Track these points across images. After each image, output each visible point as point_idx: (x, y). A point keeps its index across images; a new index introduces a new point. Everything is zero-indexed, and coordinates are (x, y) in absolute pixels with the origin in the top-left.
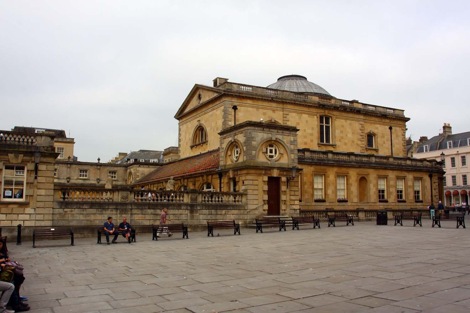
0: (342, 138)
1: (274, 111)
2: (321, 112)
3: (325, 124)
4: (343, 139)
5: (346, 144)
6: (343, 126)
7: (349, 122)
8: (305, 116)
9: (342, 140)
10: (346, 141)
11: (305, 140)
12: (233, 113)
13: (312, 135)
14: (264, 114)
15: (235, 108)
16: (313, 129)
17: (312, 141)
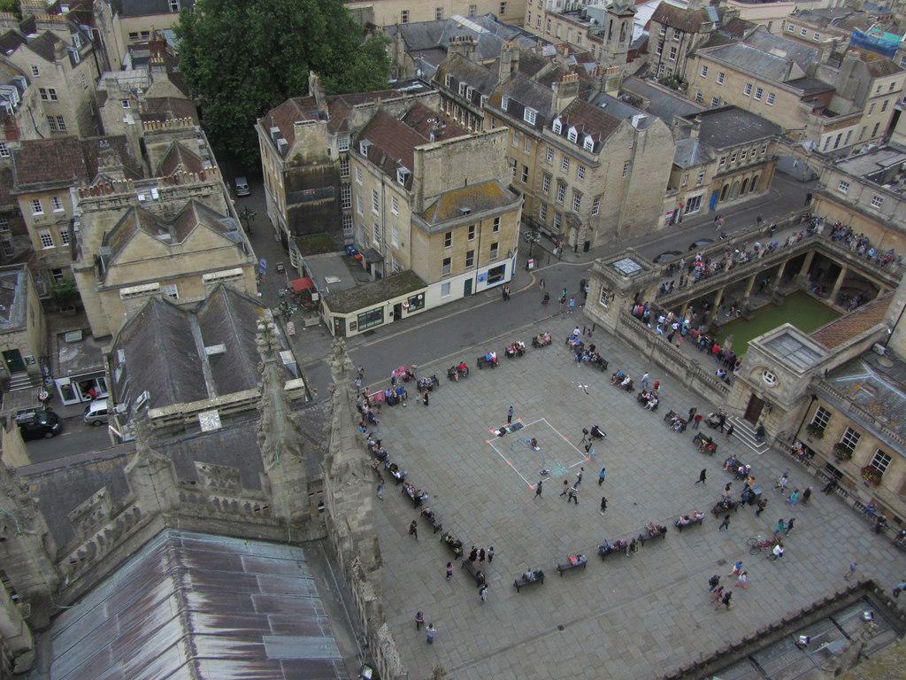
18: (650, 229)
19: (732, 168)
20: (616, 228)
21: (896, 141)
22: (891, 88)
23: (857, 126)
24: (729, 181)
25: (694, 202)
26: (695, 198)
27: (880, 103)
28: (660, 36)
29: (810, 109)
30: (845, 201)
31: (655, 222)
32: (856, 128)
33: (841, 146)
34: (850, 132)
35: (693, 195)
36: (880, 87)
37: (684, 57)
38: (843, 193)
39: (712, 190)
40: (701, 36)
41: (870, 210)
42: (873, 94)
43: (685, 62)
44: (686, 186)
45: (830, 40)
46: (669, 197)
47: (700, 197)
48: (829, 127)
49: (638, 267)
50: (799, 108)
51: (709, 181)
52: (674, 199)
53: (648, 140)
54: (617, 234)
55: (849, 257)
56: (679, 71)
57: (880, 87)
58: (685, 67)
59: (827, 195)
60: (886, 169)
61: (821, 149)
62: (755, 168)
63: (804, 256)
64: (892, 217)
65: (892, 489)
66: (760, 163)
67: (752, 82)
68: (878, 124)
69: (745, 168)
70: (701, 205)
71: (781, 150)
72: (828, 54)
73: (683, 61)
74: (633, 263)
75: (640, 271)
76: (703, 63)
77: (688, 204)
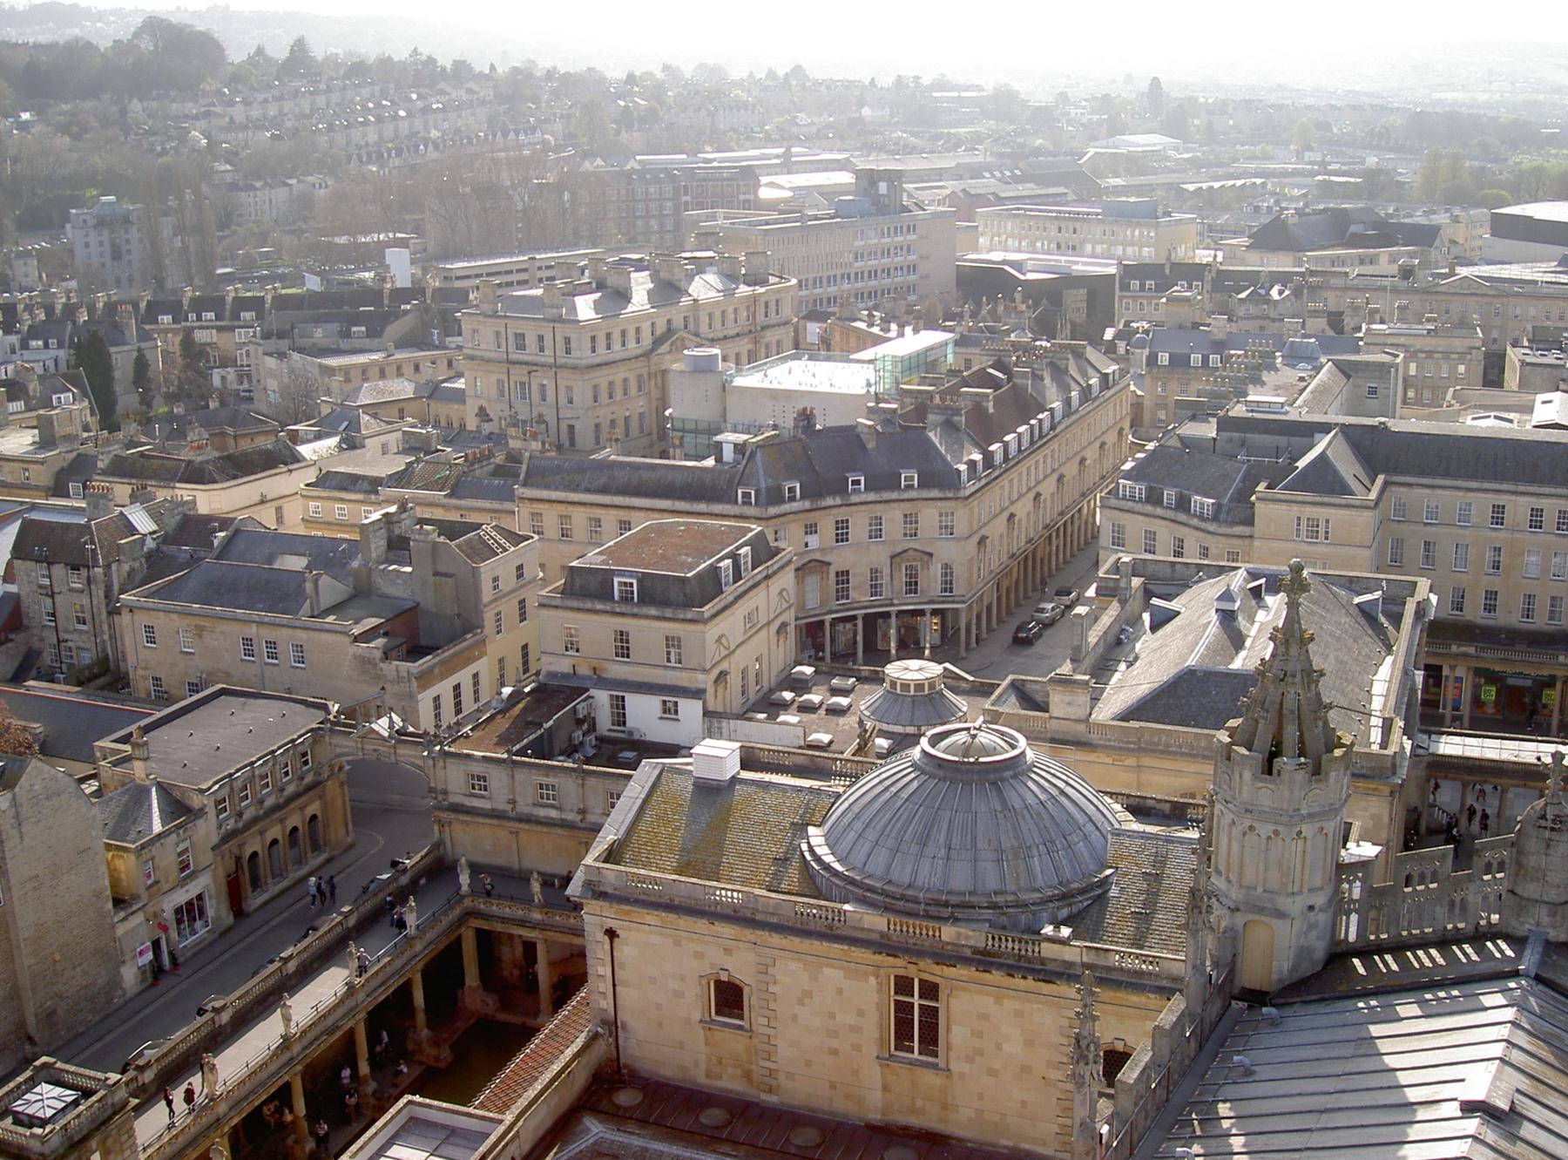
1: (728, 951)
2: (899, 965)
3: (920, 997)
4: (982, 1055)
5: (992, 1072)
6: (984, 1017)
7: (1010, 1005)
8: (833, 974)
9: (978, 1059)
10: (997, 1065)
11: (835, 1043)
12: (607, 947)
13: (857, 1029)
14: (699, 955)
15: (611, 934)
16: (861, 1013)
17: (857, 1047)
18: (109, 1001)
19: (247, 815)
20: (22, 1024)
21: (552, 668)
22: (520, 576)
23: (485, 659)
24: (254, 845)
25: (191, 912)
26: (190, 904)
27: (509, 608)
28: (41, 587)
29: (378, 654)
30: (493, 810)
31: (115, 982)
32: (484, 666)
33: (469, 706)
34: (476, 676)
35: (182, 897)
36: (495, 579)
37: (104, 614)
38: (483, 797)
39: (221, 874)
40: (126, 567)
41: (542, 812)
42: (487, 593)
43: (111, 626)
44: (157, 882)
45: (376, 516)
46: (125, 919)
47: (200, 897)
48: (425, 679)
49: (70, 1095)
50: (355, 657)
51: (207, 857)
52: (139, 918)
53: (24, 810)
54: (30, 1039)
55: (537, 916)
56: (104, 649)
57: (495, 579)
58: (113, 637)
59: (457, 809)
60: (546, 726)
61: (427, 722)
62: (304, 798)
63: (455, 947)
64: (583, 812)
66: (309, 789)
67: (252, 630)
68: (525, 647)
69: (277, 808)
70: (210, 912)
71: (338, 750)
72: (383, 543)
73: (105, 628)
74: (58, 1091)
75: (76, 1103)
76: (142, 619)
77: (179, 921)
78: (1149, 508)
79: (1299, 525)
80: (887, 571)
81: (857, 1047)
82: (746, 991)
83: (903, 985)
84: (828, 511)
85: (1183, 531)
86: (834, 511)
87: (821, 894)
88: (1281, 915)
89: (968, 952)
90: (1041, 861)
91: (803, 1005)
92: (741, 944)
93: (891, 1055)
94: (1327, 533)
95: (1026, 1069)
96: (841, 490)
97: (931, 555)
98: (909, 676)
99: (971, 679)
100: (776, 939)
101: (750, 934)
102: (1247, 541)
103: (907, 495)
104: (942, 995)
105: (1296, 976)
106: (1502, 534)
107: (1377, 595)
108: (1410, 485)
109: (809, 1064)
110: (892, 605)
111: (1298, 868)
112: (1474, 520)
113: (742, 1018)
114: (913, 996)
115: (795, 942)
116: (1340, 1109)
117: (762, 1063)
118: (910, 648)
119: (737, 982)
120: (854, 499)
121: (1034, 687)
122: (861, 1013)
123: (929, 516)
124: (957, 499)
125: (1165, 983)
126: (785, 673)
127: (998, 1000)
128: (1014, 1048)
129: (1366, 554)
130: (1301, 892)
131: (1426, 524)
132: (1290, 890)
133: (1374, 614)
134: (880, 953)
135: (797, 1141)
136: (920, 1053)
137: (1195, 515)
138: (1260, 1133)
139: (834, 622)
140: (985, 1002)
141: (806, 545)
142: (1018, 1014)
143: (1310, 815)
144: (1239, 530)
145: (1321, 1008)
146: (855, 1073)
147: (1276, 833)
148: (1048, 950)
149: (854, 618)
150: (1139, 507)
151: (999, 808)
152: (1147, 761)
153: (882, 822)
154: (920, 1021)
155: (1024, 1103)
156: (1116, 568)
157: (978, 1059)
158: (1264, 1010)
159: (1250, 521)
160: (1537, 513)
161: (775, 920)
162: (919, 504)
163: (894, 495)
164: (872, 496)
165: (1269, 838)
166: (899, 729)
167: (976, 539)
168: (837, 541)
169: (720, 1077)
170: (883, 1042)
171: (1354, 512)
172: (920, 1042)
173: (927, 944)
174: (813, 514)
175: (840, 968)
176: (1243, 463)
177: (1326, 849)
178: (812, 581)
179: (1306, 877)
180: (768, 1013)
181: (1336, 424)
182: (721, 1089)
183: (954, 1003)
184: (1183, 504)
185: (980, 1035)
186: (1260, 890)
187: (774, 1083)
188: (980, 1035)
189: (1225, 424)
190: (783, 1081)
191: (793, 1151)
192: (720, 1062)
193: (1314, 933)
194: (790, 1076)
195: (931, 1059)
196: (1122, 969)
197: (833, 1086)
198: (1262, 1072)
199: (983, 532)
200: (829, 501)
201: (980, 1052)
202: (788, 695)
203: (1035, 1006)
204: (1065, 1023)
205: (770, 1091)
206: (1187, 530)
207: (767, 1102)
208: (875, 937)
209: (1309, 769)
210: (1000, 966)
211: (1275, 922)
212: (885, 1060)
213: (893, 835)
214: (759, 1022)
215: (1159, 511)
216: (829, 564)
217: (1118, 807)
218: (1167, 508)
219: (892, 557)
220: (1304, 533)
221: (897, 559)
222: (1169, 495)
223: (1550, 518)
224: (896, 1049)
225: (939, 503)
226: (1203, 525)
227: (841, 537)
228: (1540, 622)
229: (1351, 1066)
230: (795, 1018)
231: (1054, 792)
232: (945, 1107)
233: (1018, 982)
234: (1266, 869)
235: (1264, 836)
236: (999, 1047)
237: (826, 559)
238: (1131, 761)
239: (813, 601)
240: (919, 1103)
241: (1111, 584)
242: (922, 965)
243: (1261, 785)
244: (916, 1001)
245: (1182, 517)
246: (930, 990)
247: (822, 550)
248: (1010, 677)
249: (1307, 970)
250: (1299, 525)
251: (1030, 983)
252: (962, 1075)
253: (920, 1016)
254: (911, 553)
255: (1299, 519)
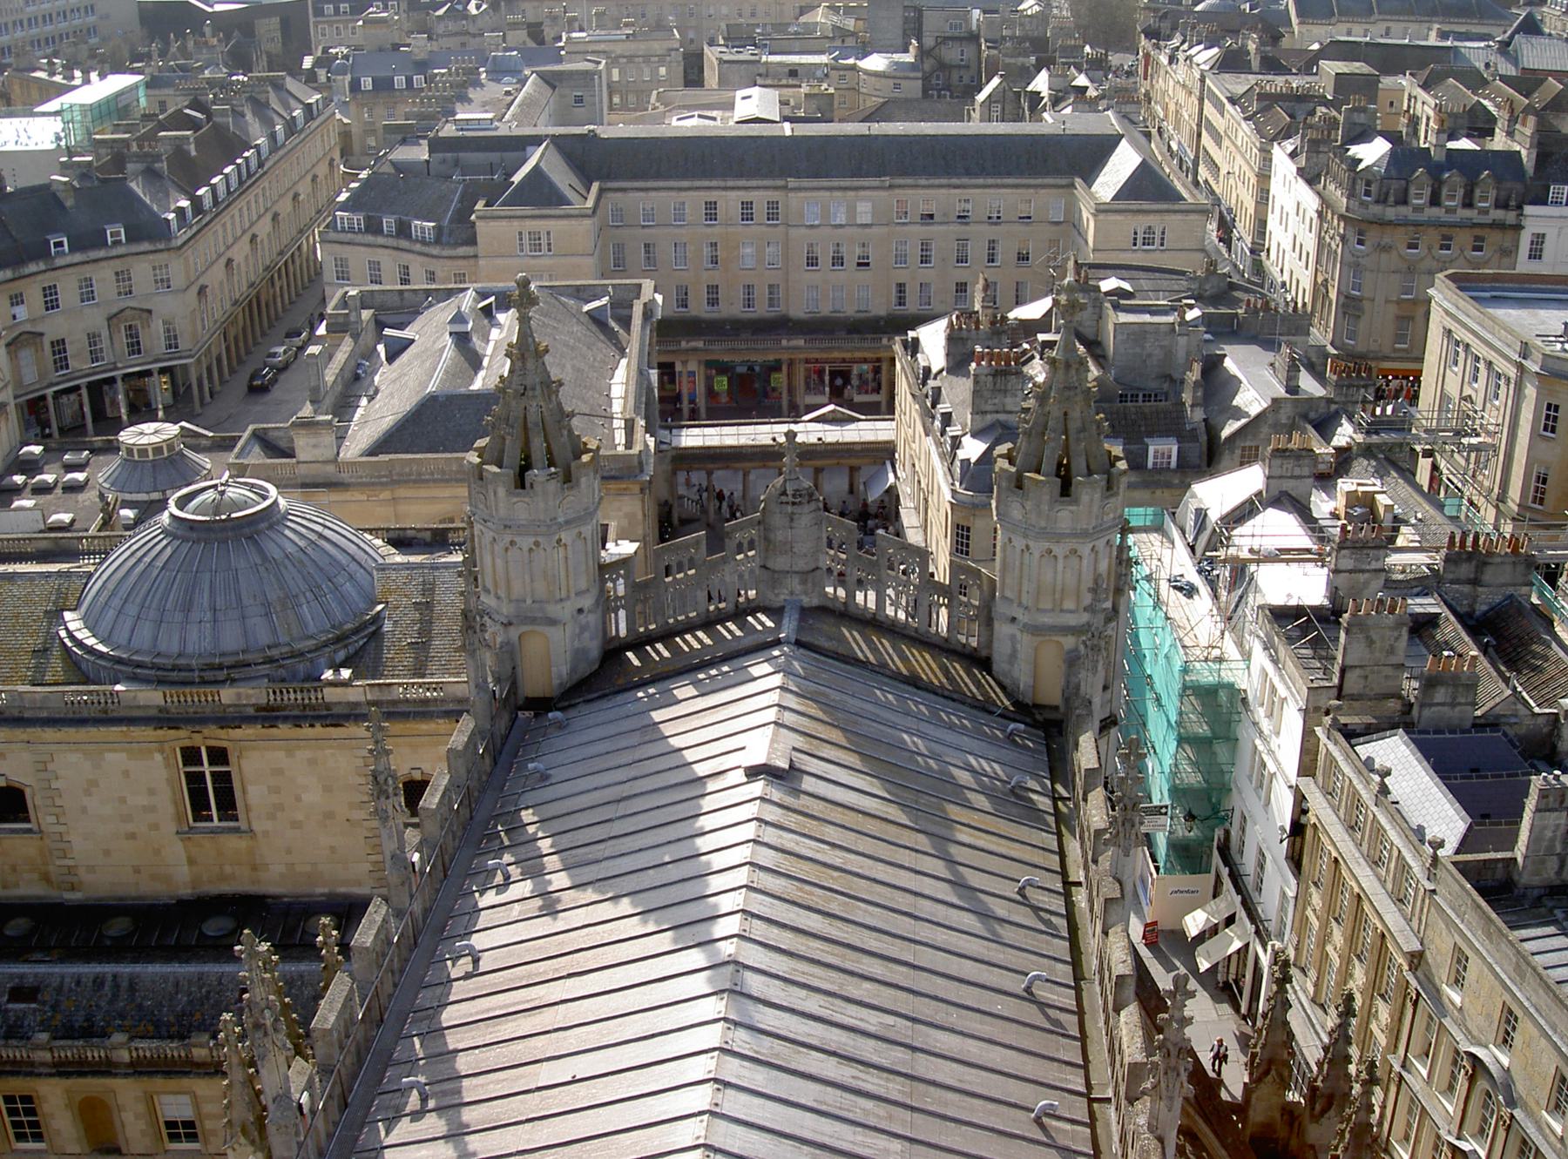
0: (280, 807)
3: (211, 764)
5: (296, 825)
6: (279, 772)
7: (303, 755)
8: (116, 759)
9: (279, 814)
10: (300, 817)
11: (130, 827)
13: (151, 809)
16: (152, 792)
17: (155, 827)
65: (77, 1150)
78: (370, 238)
79: (521, 239)
80: (105, 333)
81: (155, 827)
82: (28, 792)
83: (191, 755)
84: (33, 278)
85: (406, 258)
86: (40, 277)
87: (88, 678)
88: (552, 622)
89: (251, 711)
90: (310, 607)
91: (90, 795)
92: (14, 746)
93: (191, 828)
94: (549, 244)
95: (329, 815)
96: (42, 253)
97: (150, 312)
98: (144, 440)
99: (211, 434)
100: (49, 734)
101: (20, 734)
102: (472, 261)
103: (114, 252)
104: (232, 758)
105: (576, 678)
106: (716, 230)
107: (605, 300)
108: (624, 190)
109: (107, 853)
110: (116, 369)
111: (563, 573)
112: (688, 218)
113: (27, 820)
114: (202, 764)
115: (70, 733)
116: (635, 795)
117: (58, 862)
118: (141, 411)
119: (17, 785)
120: (59, 262)
121: (276, 434)
122: (152, 792)
123: (142, 271)
124: (169, 250)
125: (451, 707)
126: (12, 457)
127: (290, 753)
128: (313, 796)
129: (590, 262)
130: (568, 597)
131: (643, 227)
132: (558, 597)
133: (603, 319)
134: (161, 728)
135: (113, 932)
136: (220, 820)
137: (417, 241)
138: (565, 832)
139: (57, 395)
140: (278, 757)
141: (14, 317)
142: (312, 762)
143: (567, 522)
144: (462, 251)
145: (604, 704)
146: (157, 852)
147: (537, 544)
148: (331, 695)
149: (77, 388)
150: (359, 238)
151: (259, 561)
152: (402, 492)
153: (141, 596)
154: (214, 788)
155: (333, 849)
156: (344, 303)
157: (279, 814)
158: (550, 715)
159: (472, 241)
160: (747, 205)
161: (45, 714)
162: (129, 259)
163: (102, 253)
164: (78, 257)
165: (531, 550)
166: (142, 497)
167: (195, 289)
168: (47, 309)
169: (17, 885)
170: (180, 817)
171: (573, 222)
172: (218, 809)
173: (208, 710)
174: (17, 283)
175: (123, 750)
176: (459, 182)
177: (586, 552)
178: (26, 355)
179: (571, 582)
180: (57, 810)
181: (547, 136)
182: (22, 898)
183: (244, 763)
184: (403, 230)
185: (276, 790)
186: (529, 601)
187: (74, 879)
188: (276, 790)
189: (437, 145)
190: (82, 872)
191: (108, 943)
192: (14, 869)
193: (587, 635)
194: (91, 869)
195: (232, 824)
196: (407, 700)
197: (137, 870)
198: (558, 775)
199: (201, 281)
200: (32, 268)
201: (280, 807)
202: (19, 479)
203: (328, 752)
204: (360, 762)
205: (73, 888)
206: (411, 256)
207: (70, 900)
208: (153, 713)
209: (561, 478)
210: (286, 719)
211: (550, 631)
212: (185, 833)
213: (154, 605)
214: (47, 821)
215: (380, 240)
216: (42, 334)
217: (379, 542)
218: (387, 236)
219: (109, 319)
220: (527, 247)
221: (115, 320)
222: (388, 222)
223: (760, 210)
224: (195, 821)
225: (151, 257)
226: (426, 249)
227: (52, 305)
228: (761, 310)
229: (638, 754)
230: (84, 810)
231: (313, 537)
232: (254, 868)
233: (306, 731)
234: (532, 581)
235: (525, 549)
236: (298, 799)
237: (39, 329)
238: (386, 495)
239: (30, 376)
240: (228, 869)
241: (341, 320)
242: (206, 732)
243: (515, 500)
244: (207, 768)
245: (404, 244)
246: (219, 756)
247: (33, 321)
248: (251, 428)
249: (585, 670)
250: (521, 239)
251: (318, 730)
252: (266, 833)
253: (213, 783)
254: (128, 312)
255: (520, 233)
